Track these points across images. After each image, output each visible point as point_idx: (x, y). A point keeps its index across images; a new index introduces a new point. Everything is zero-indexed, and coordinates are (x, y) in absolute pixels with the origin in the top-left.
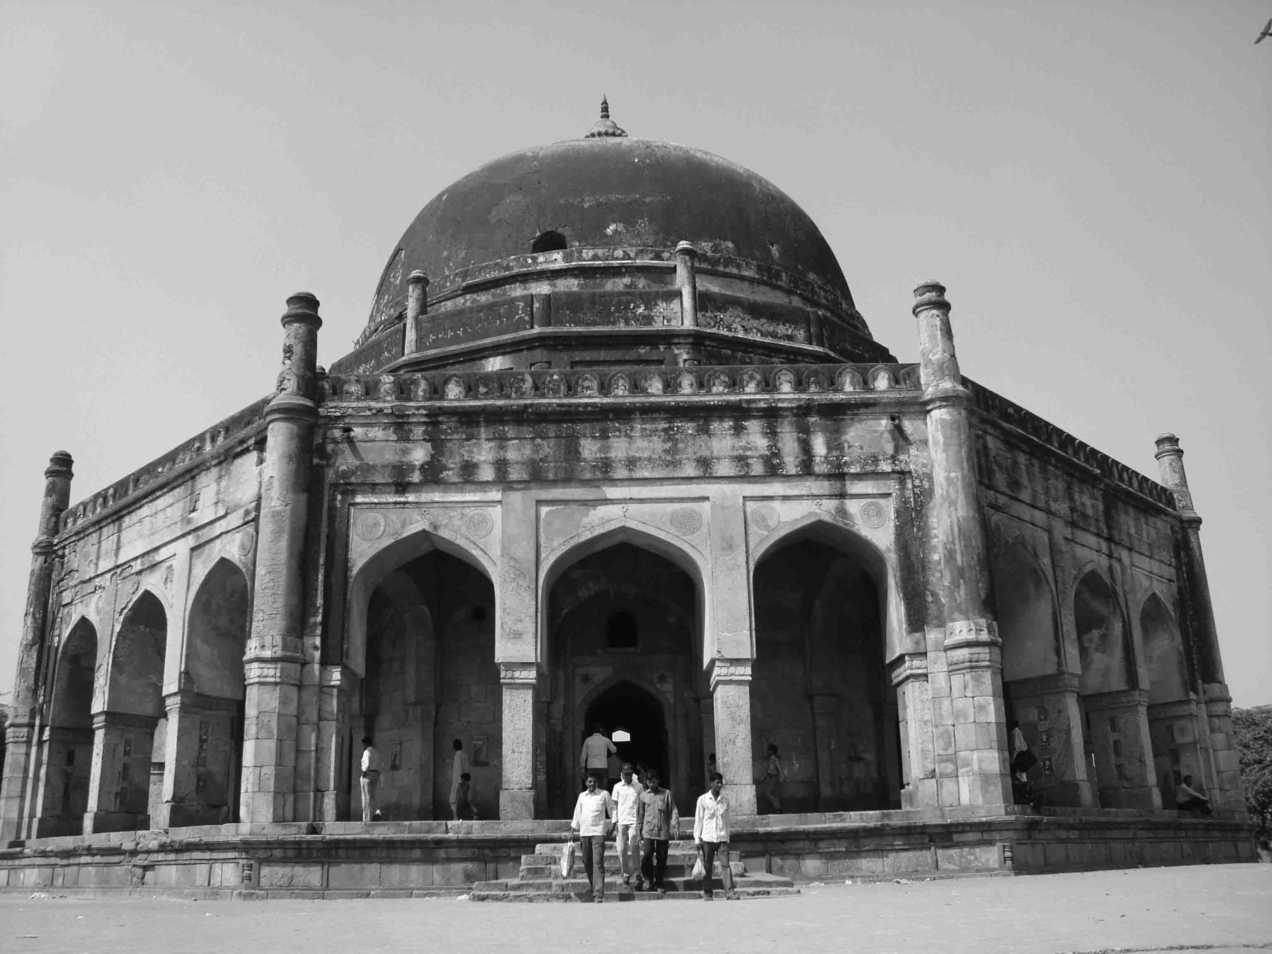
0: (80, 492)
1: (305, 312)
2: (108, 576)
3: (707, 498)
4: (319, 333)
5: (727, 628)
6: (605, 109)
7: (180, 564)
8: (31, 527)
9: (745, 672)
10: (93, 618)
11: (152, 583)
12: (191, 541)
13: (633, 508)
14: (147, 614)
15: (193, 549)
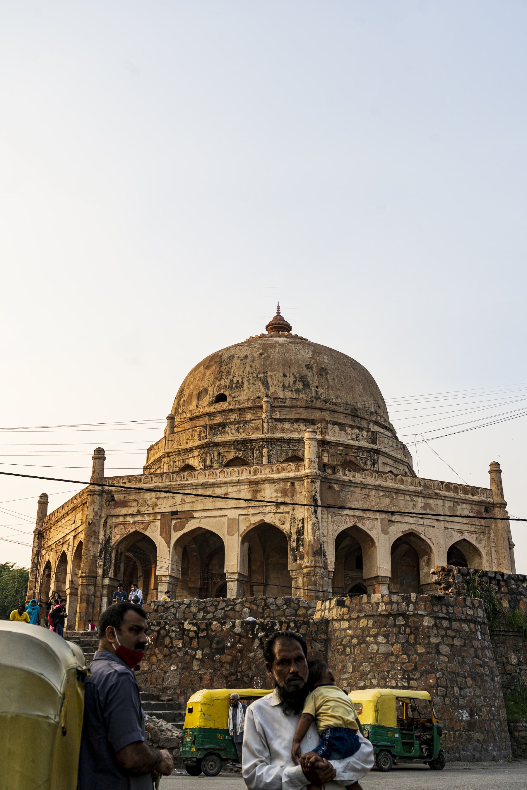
0: (51, 509)
1: (100, 455)
2: (55, 544)
3: (226, 515)
4: (105, 462)
5: (233, 562)
6: (278, 308)
7: (71, 541)
8: (31, 526)
9: (236, 576)
10: (51, 561)
11: (65, 548)
12: (73, 534)
13: (203, 520)
14: (63, 559)
15: (74, 536)
